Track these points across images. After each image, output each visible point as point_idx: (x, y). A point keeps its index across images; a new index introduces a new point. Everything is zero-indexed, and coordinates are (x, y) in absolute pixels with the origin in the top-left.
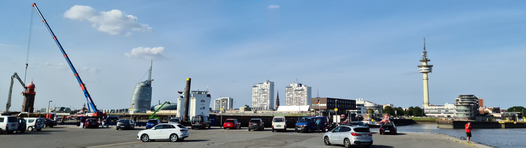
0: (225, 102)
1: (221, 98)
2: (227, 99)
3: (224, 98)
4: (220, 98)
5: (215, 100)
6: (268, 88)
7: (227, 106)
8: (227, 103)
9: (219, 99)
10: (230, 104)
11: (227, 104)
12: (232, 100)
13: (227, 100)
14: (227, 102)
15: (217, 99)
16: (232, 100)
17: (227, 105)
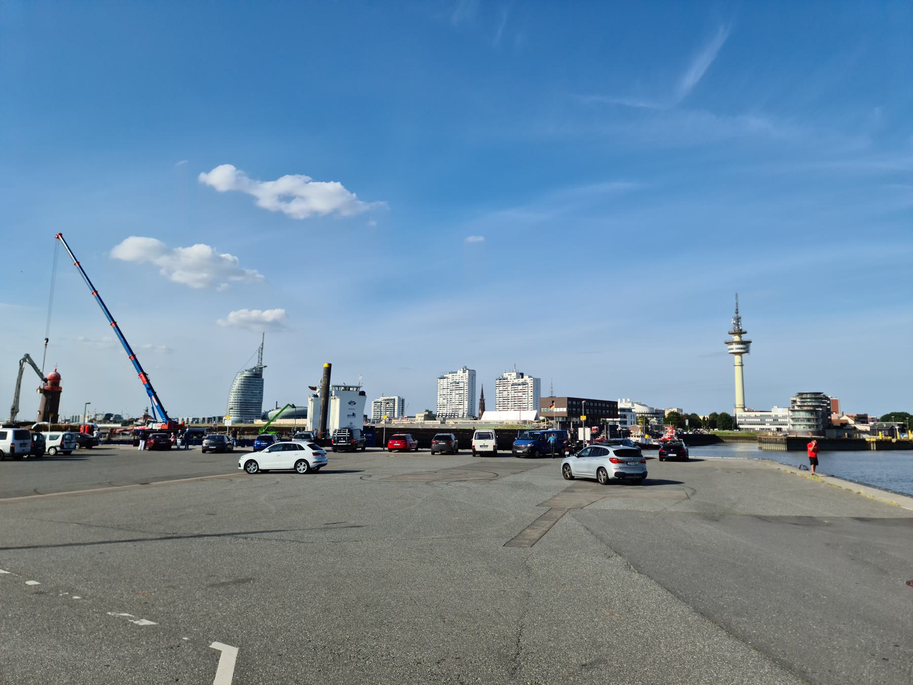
0: (391, 404)
1: (384, 398)
2: (394, 400)
3: (388, 398)
4: (381, 398)
5: (373, 402)
6: (464, 380)
7: (394, 411)
8: (394, 406)
9: (379, 400)
10: (399, 408)
11: (394, 408)
12: (403, 400)
13: (394, 402)
14: (394, 404)
15: (376, 400)
16: (402, 402)
17: (394, 409)
